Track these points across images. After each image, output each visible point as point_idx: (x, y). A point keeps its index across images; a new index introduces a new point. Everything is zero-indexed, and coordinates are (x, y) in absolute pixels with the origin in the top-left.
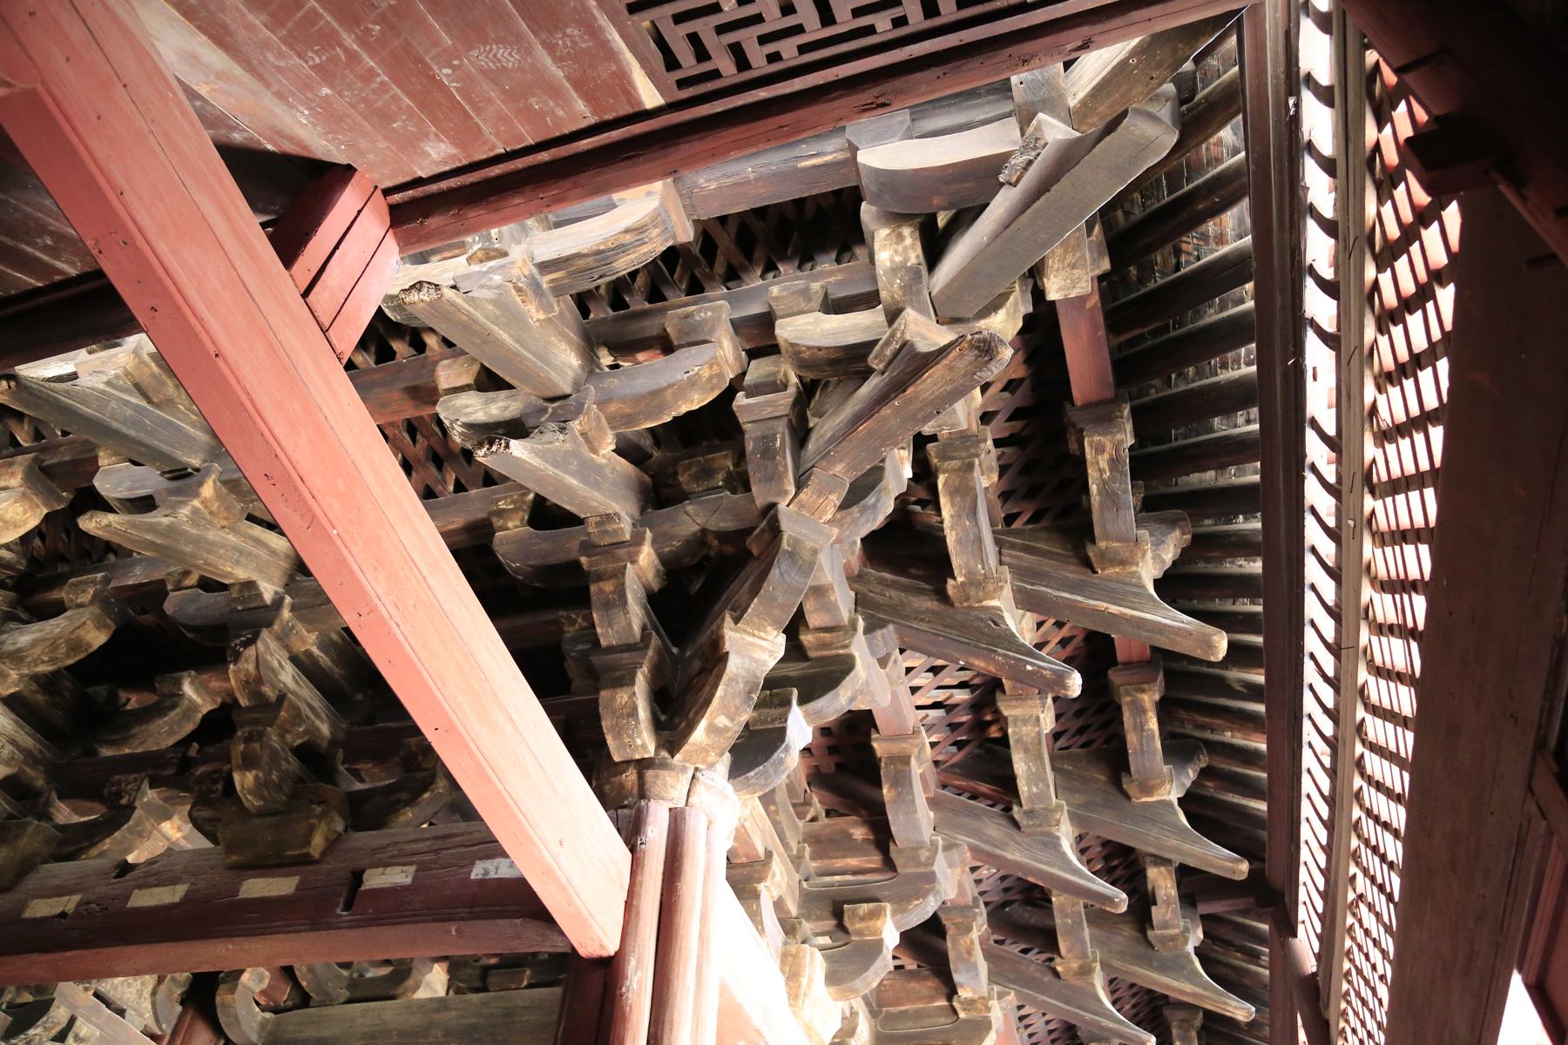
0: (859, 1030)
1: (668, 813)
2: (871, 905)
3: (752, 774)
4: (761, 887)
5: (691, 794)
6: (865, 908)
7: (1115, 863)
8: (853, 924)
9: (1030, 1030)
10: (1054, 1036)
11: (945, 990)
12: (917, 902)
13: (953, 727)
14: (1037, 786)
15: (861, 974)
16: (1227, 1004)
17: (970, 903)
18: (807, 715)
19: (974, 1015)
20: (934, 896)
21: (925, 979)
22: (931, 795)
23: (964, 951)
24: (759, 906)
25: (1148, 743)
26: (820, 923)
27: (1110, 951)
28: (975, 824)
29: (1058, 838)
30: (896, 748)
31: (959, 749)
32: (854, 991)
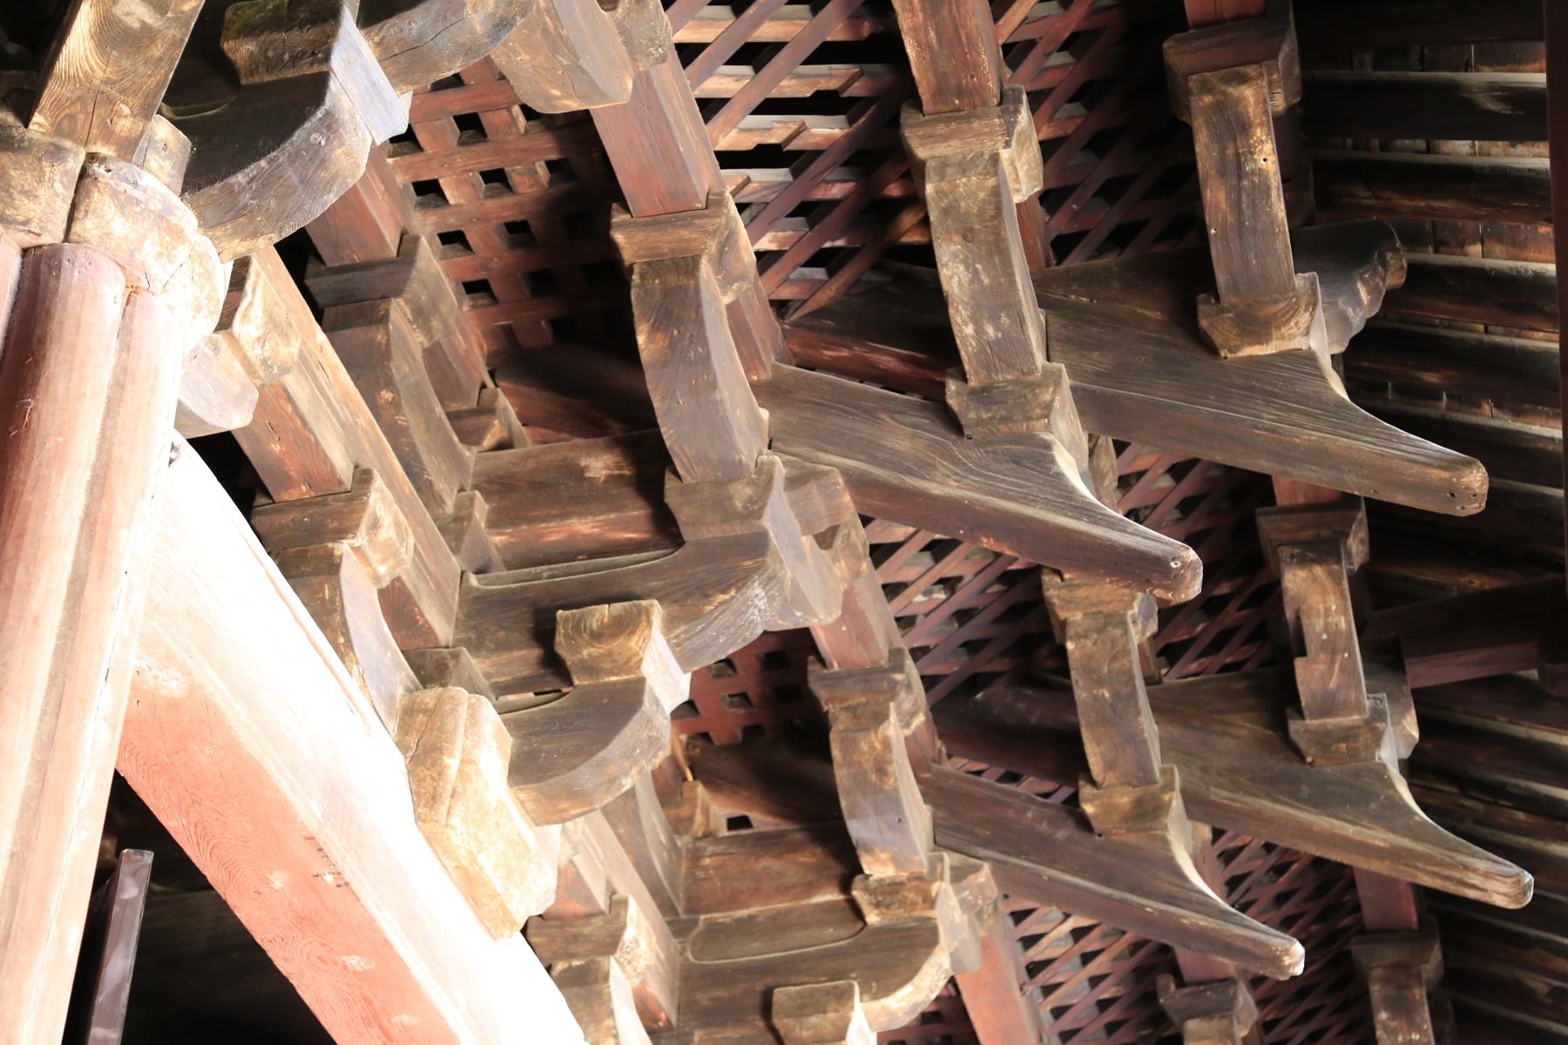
0: (628, 935)
1: (16, 262)
2: (618, 607)
3: (240, 178)
4: (343, 548)
5: (80, 215)
6: (603, 612)
7: (1224, 589)
8: (576, 649)
9: (1056, 999)
10: (1111, 1015)
11: (837, 869)
12: (722, 597)
13: (809, 211)
14: (998, 328)
15: (591, 754)
16: (1466, 868)
17: (884, 663)
18: (387, 56)
19: (898, 916)
20: (765, 585)
21: (795, 848)
22: (766, 375)
23: (868, 766)
24: (336, 588)
25: (1253, 206)
26: (504, 657)
27: (1204, 770)
28: (863, 429)
29: (1048, 446)
30: (666, 241)
31: (831, 273)
32: (580, 798)
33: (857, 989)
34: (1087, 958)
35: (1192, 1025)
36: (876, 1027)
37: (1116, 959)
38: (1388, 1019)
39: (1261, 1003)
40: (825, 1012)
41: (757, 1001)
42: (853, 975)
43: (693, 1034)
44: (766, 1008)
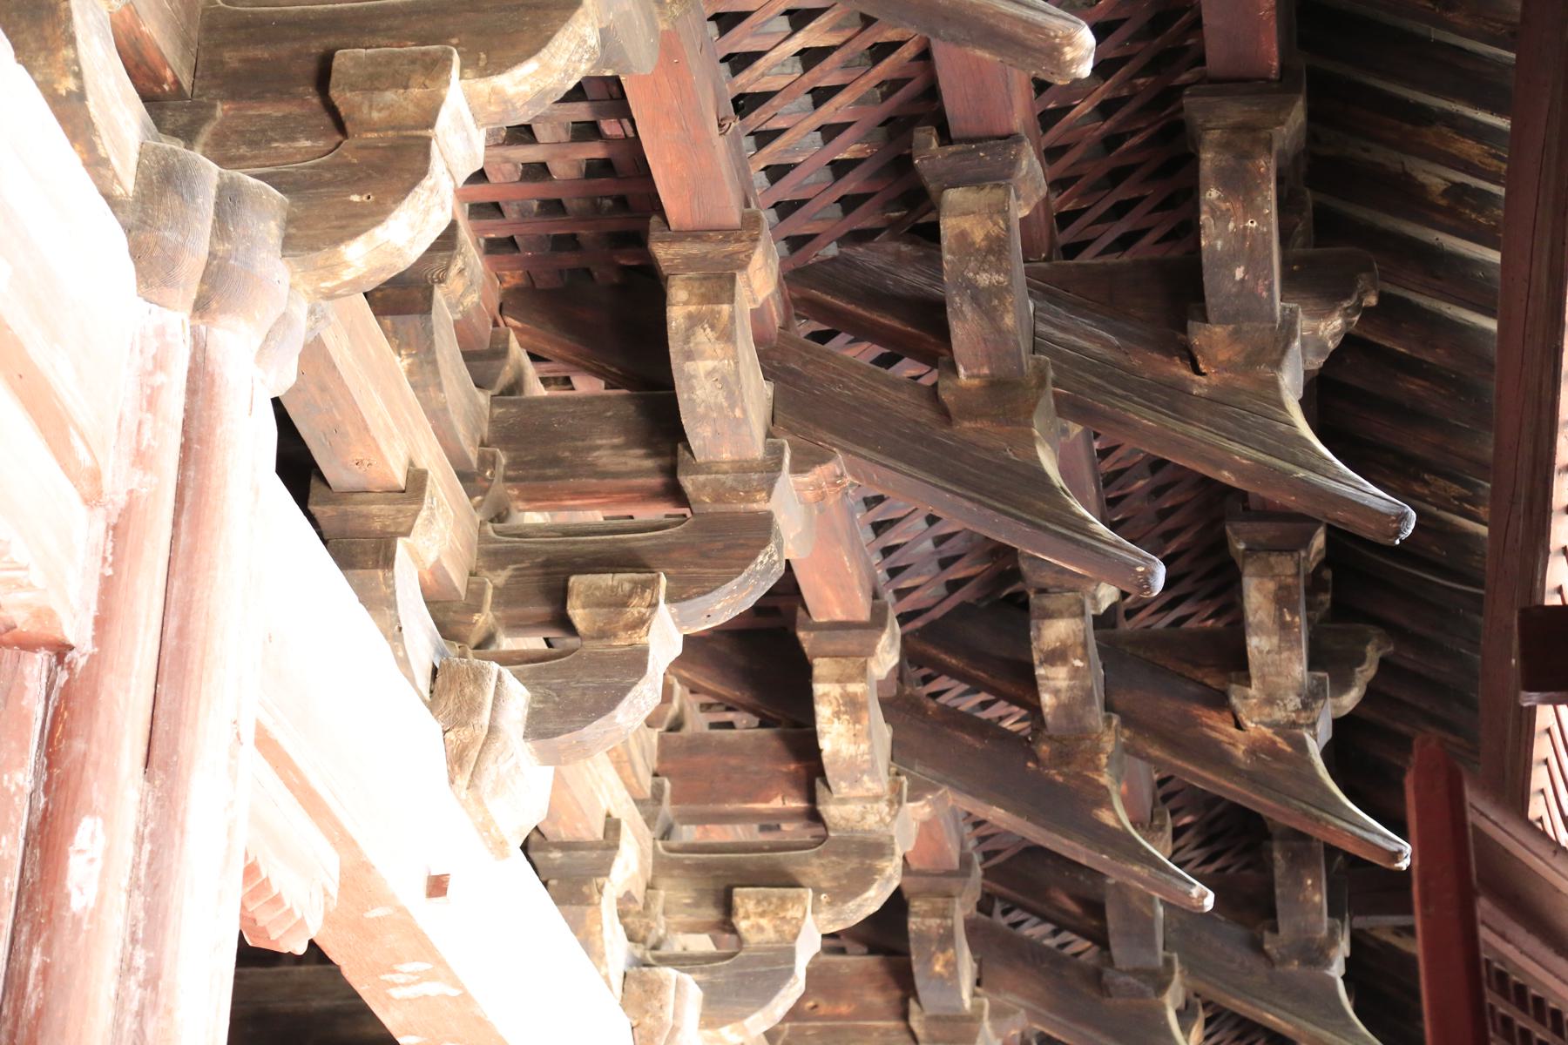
9: (773, 153)
10: (851, 184)
33: (456, 59)
34: (821, 96)
35: (953, 195)
36: (484, 121)
37: (860, 102)
38: (1219, 198)
39: (1057, 185)
40: (406, 87)
41: (311, 67)
42: (455, 41)
43: (214, 106)
44: (323, 78)
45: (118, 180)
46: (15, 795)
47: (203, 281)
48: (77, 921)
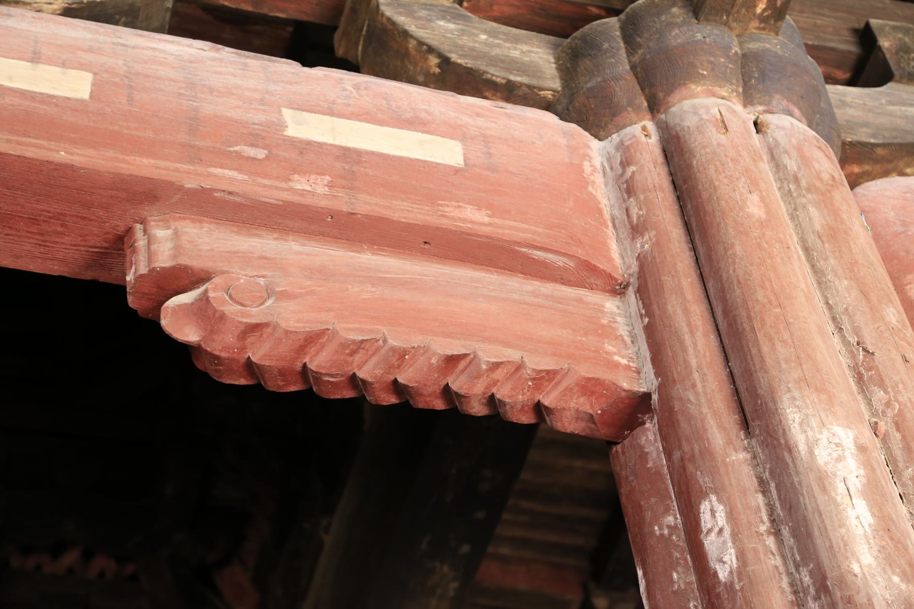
45: (535, 87)
46: (670, 535)
47: (643, 89)
48: (730, 587)
